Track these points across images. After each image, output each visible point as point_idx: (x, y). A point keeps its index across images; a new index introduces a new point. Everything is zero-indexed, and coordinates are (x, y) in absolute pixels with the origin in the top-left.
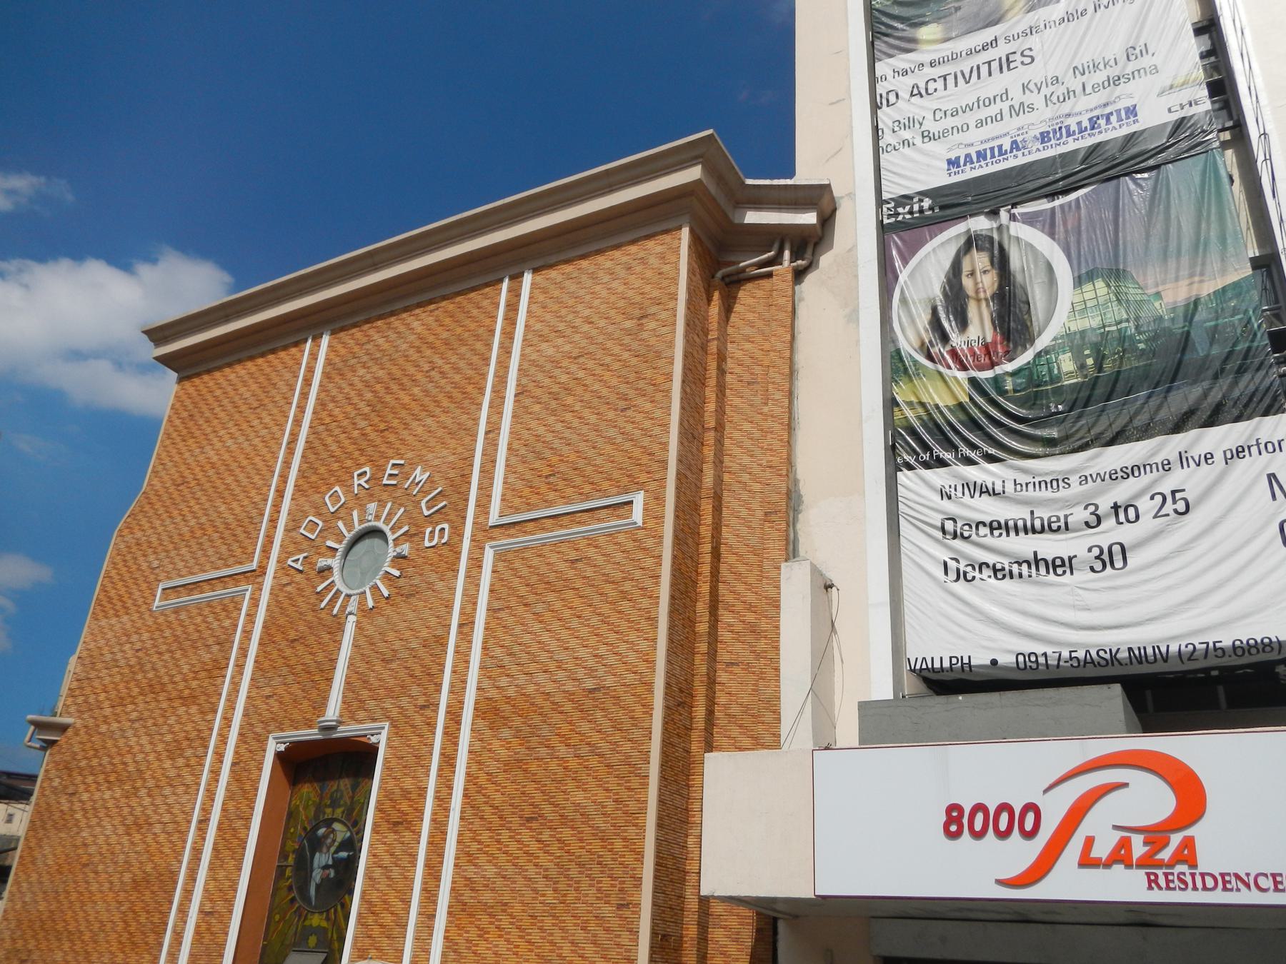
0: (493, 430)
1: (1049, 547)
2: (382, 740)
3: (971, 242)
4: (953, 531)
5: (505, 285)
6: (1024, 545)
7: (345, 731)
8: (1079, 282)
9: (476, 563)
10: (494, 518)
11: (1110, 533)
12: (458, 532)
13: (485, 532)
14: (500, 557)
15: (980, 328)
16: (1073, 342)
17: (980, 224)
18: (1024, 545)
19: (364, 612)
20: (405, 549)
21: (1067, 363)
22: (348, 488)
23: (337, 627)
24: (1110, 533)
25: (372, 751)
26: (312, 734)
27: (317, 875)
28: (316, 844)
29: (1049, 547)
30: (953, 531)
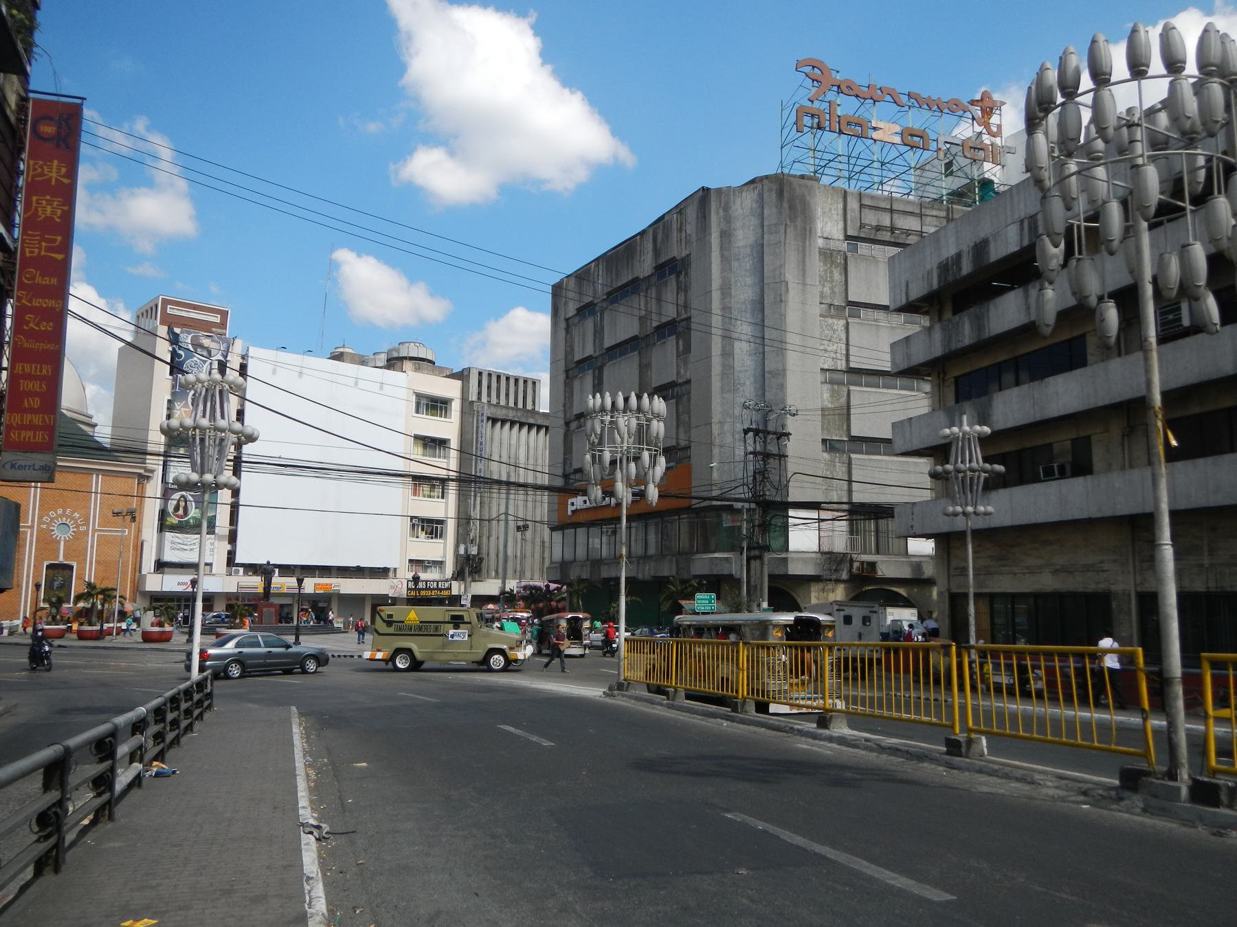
0: (95, 509)
1: (185, 547)
2: (75, 564)
3: (183, 496)
4: (173, 543)
5: (94, 476)
6: (182, 546)
7: (65, 562)
8: (196, 508)
9: (93, 536)
10: (96, 528)
11: (192, 547)
12: (88, 529)
13: (94, 530)
14: (98, 535)
15: (181, 512)
16: (193, 518)
17: (184, 493)
18: (182, 546)
19: (66, 541)
20: (75, 530)
21: (191, 521)
22: (56, 513)
23: (59, 542)
24: (192, 547)
25: (73, 567)
26: (57, 562)
27: (55, 586)
28: (55, 581)
29: (185, 547)
30: (173, 543)
